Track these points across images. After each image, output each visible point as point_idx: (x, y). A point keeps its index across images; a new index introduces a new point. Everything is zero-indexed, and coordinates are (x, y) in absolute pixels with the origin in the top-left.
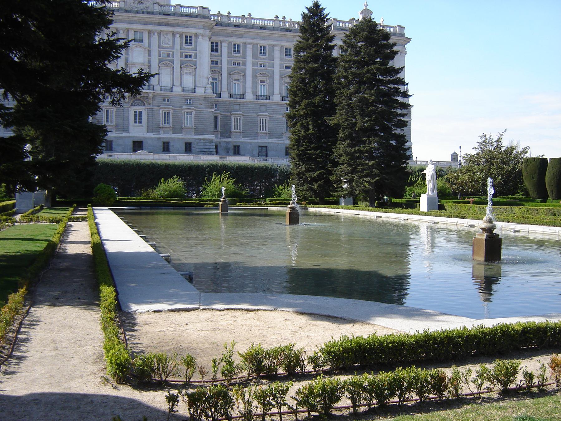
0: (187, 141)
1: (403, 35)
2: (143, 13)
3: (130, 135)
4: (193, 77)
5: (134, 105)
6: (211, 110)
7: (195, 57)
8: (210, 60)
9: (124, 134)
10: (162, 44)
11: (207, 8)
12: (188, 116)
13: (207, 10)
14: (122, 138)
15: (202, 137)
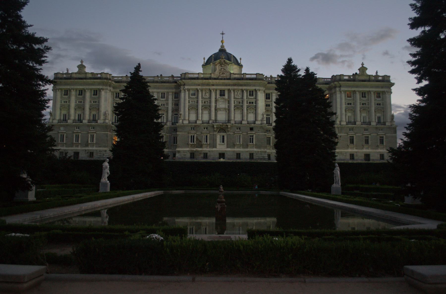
0: (251, 152)
1: (389, 81)
2: (225, 79)
3: (217, 150)
4: (254, 115)
5: (220, 132)
6: (265, 134)
7: (256, 103)
8: (264, 104)
9: (214, 149)
10: (235, 97)
11: (262, 74)
12: (251, 137)
13: (262, 75)
14: (212, 151)
15: (259, 150)
